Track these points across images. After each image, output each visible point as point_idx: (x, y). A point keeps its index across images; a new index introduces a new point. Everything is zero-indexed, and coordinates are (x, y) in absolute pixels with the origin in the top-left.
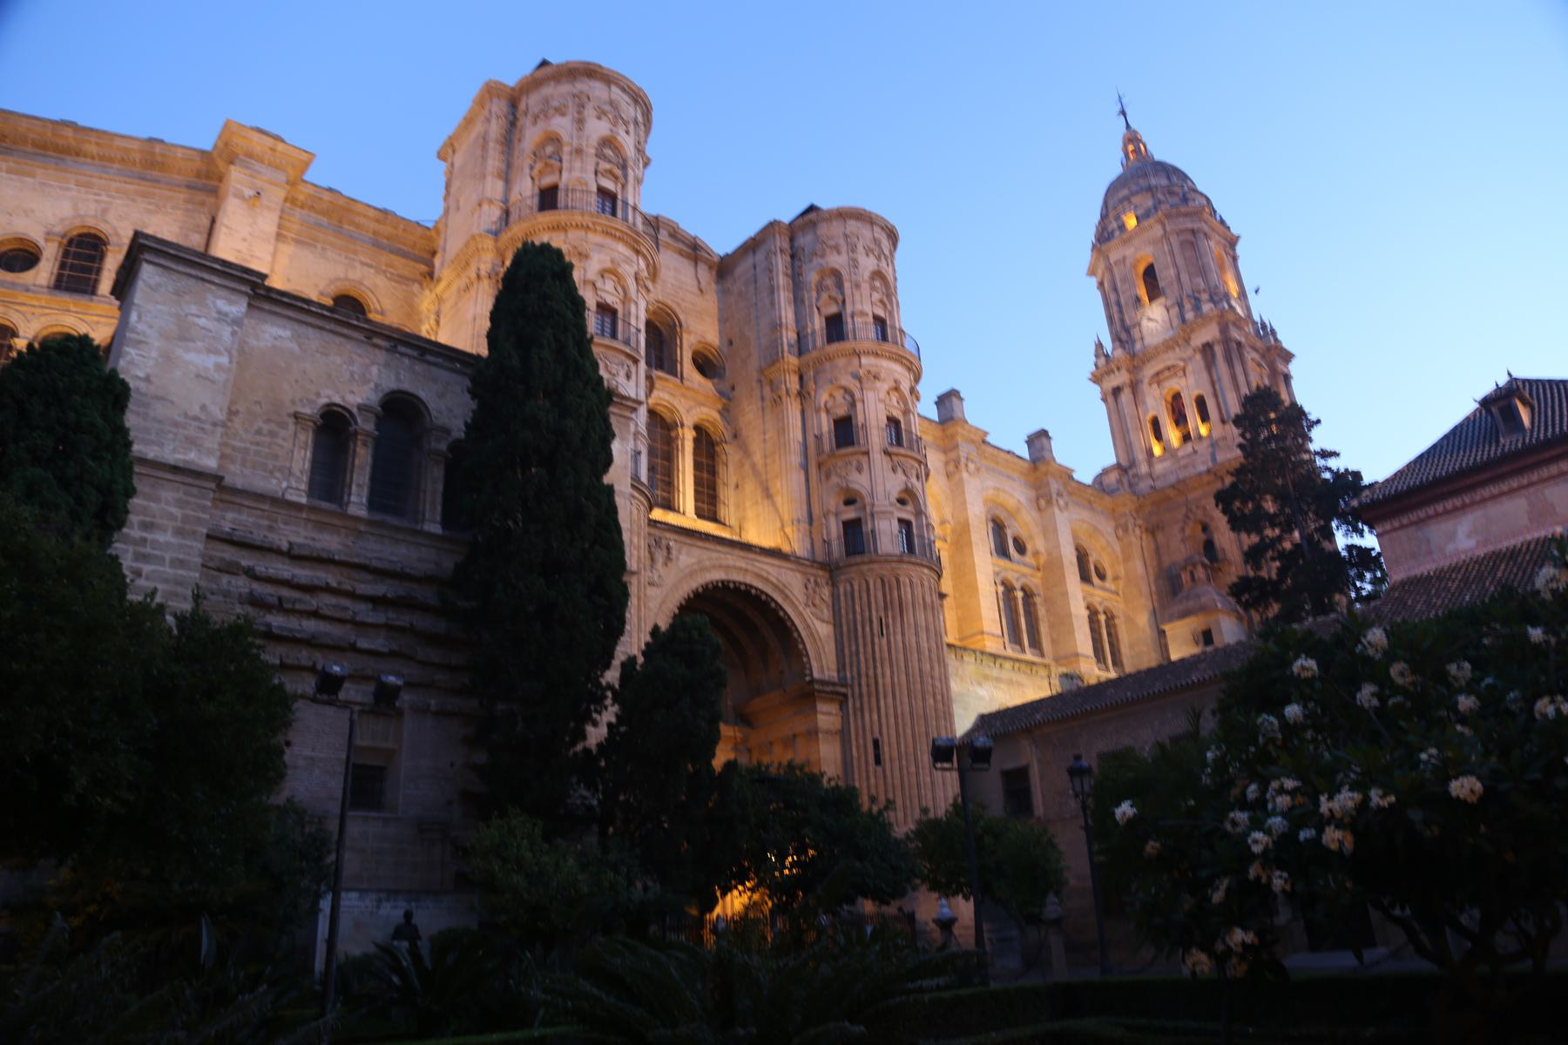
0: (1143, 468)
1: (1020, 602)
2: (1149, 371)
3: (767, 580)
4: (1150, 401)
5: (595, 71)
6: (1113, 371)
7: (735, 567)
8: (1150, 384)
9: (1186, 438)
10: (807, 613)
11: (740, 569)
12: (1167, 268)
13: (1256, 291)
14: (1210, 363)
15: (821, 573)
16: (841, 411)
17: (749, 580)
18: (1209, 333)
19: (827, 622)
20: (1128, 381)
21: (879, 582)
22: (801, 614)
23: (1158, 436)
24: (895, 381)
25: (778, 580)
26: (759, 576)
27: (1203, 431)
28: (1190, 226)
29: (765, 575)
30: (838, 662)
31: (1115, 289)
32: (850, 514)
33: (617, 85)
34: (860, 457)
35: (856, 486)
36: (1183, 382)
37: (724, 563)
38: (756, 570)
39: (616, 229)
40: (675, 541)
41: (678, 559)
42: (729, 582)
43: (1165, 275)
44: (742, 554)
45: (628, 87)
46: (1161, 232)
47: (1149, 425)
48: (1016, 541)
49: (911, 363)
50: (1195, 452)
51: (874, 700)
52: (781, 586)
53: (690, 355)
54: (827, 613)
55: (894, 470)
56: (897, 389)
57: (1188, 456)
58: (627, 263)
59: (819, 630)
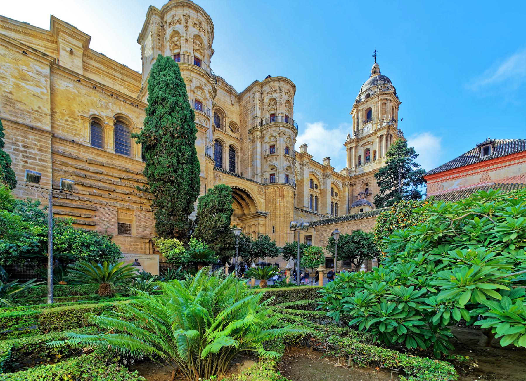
22: (256, 196)
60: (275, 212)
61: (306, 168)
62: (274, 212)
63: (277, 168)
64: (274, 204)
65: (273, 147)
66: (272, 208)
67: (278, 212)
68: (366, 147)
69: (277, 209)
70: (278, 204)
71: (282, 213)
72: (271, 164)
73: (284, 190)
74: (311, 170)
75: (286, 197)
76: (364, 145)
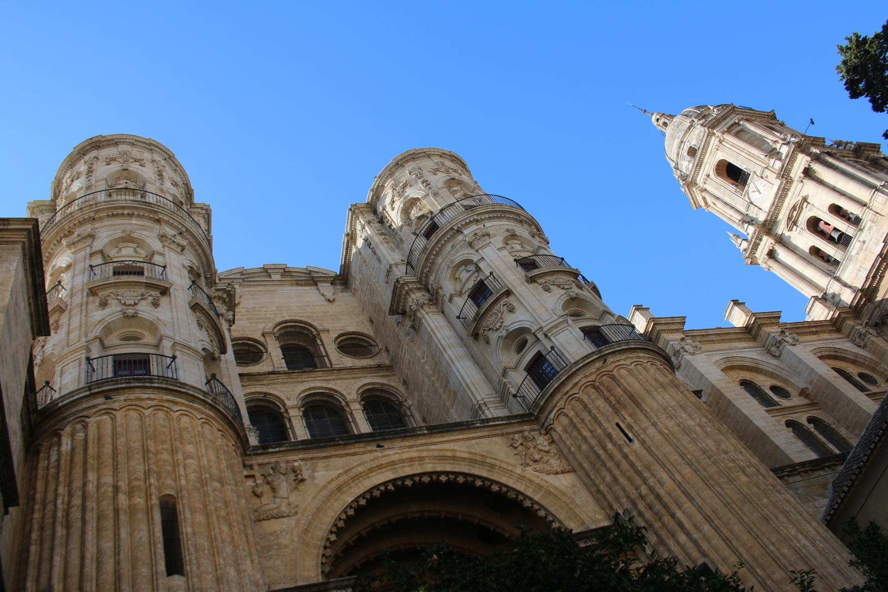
1: (816, 433)
3: (454, 458)
5: (100, 142)
6: (758, 244)
7: (402, 461)
10: (529, 472)
11: (411, 460)
13: (812, 123)
15: (525, 427)
16: (470, 284)
17: (429, 468)
18: (802, 161)
19: (563, 472)
20: (773, 241)
21: (591, 391)
22: (522, 477)
24: (508, 231)
25: (470, 453)
26: (443, 458)
28: (732, 122)
29: (449, 454)
30: (603, 508)
32: (530, 355)
33: (123, 143)
34: (504, 300)
35: (517, 326)
37: (384, 461)
38: (436, 454)
39: (123, 208)
40: (302, 460)
41: (313, 478)
42: (403, 479)
44: (406, 443)
45: (136, 141)
48: (774, 388)
49: (519, 215)
50: (864, 242)
51: (667, 519)
52: (478, 458)
53: (334, 346)
54: (556, 463)
55: (548, 290)
56: (513, 236)
57: (861, 249)
58: (145, 230)
59: (557, 484)
60: (652, 489)
61: (693, 354)
62: (644, 490)
63: (534, 328)
64: (618, 456)
65: (479, 292)
66: (621, 480)
67: (664, 476)
68: (803, 220)
69: (648, 469)
70: (636, 445)
71: (687, 471)
72: (504, 333)
73: (613, 377)
74: (718, 357)
75: (646, 396)
76: (792, 222)
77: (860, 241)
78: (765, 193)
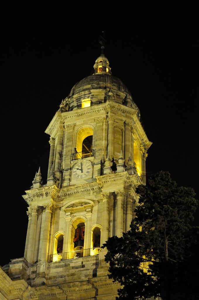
0: (42, 268)
2: (67, 202)
4: (61, 223)
6: (42, 195)
8: (65, 212)
9: (79, 255)
12: (101, 139)
14: (112, 207)
23: (60, 249)
27: (94, 252)
31: (62, 144)
36: (89, 215)
43: (99, 144)
46: (105, 116)
47: (56, 240)
50: (83, 266)
77: (82, 263)
78: (83, 176)
